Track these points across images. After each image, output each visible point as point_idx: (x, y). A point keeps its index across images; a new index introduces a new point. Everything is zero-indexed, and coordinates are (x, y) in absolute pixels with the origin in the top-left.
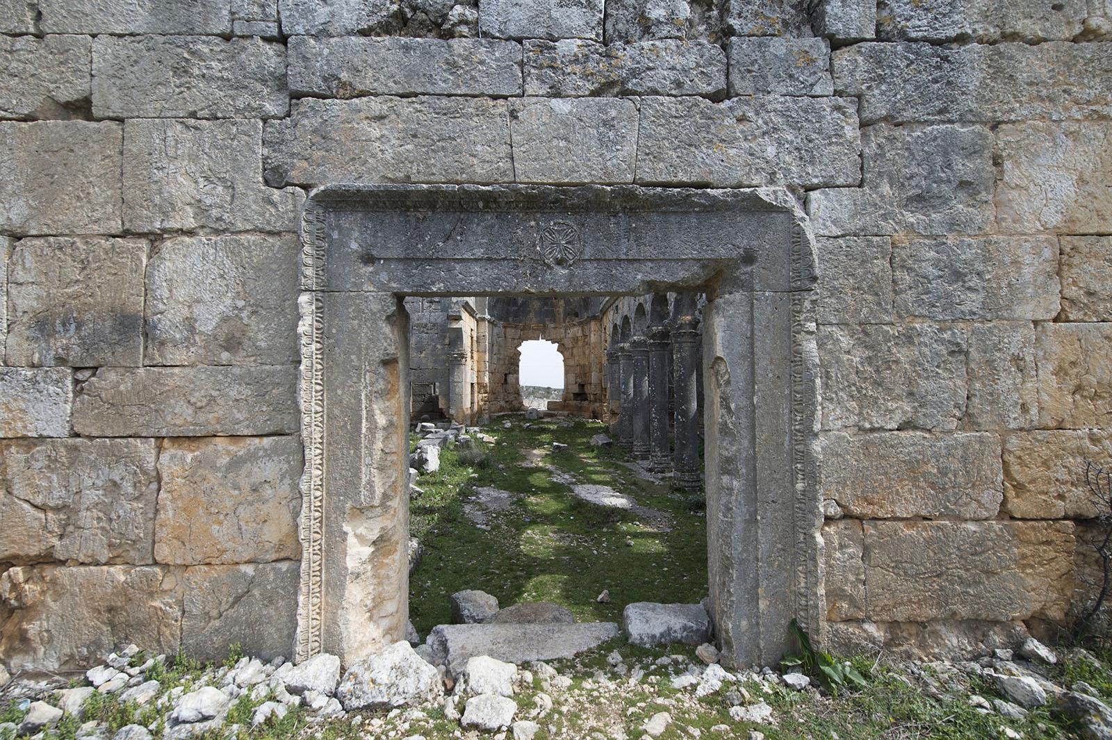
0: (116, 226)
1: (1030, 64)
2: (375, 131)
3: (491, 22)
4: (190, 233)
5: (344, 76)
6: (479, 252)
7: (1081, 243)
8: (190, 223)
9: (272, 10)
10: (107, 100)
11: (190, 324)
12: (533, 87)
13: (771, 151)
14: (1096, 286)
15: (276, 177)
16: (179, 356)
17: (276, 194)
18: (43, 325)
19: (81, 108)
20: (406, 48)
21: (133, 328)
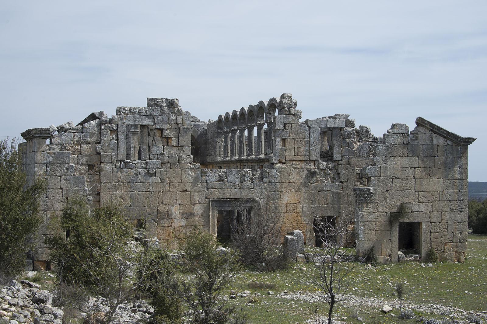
0: (190, 203)
1: (284, 185)
2: (216, 192)
3: (229, 181)
4: (197, 204)
5: (213, 187)
6: (227, 206)
7: (289, 204)
8: (198, 203)
9: (206, 180)
10: (189, 189)
11: (198, 214)
12: (233, 188)
13: (257, 194)
14: (290, 209)
15: (206, 198)
16: (197, 217)
17: (206, 200)
18: (183, 214)
19: (186, 190)
20: (220, 184)
21: (192, 214)
